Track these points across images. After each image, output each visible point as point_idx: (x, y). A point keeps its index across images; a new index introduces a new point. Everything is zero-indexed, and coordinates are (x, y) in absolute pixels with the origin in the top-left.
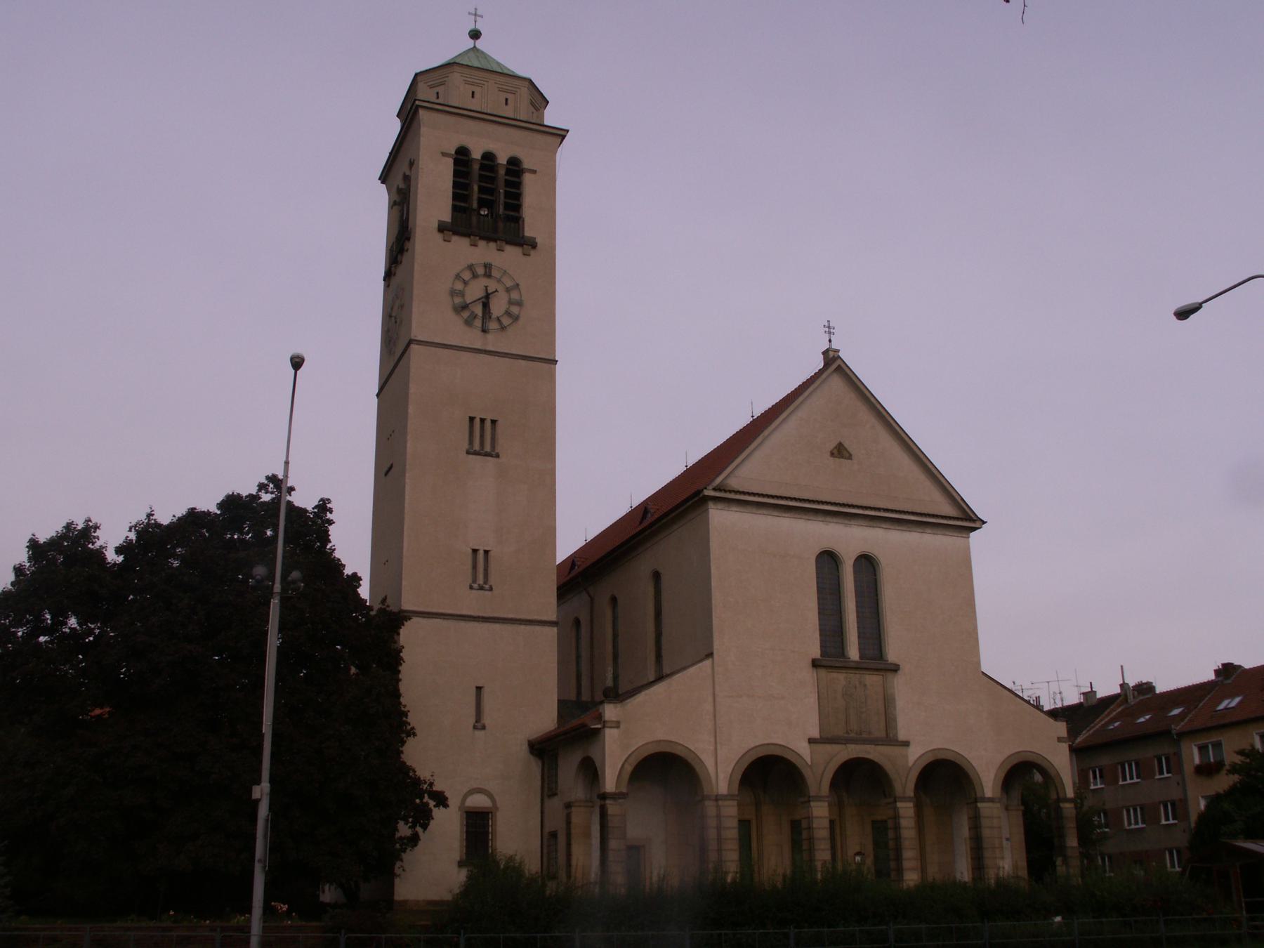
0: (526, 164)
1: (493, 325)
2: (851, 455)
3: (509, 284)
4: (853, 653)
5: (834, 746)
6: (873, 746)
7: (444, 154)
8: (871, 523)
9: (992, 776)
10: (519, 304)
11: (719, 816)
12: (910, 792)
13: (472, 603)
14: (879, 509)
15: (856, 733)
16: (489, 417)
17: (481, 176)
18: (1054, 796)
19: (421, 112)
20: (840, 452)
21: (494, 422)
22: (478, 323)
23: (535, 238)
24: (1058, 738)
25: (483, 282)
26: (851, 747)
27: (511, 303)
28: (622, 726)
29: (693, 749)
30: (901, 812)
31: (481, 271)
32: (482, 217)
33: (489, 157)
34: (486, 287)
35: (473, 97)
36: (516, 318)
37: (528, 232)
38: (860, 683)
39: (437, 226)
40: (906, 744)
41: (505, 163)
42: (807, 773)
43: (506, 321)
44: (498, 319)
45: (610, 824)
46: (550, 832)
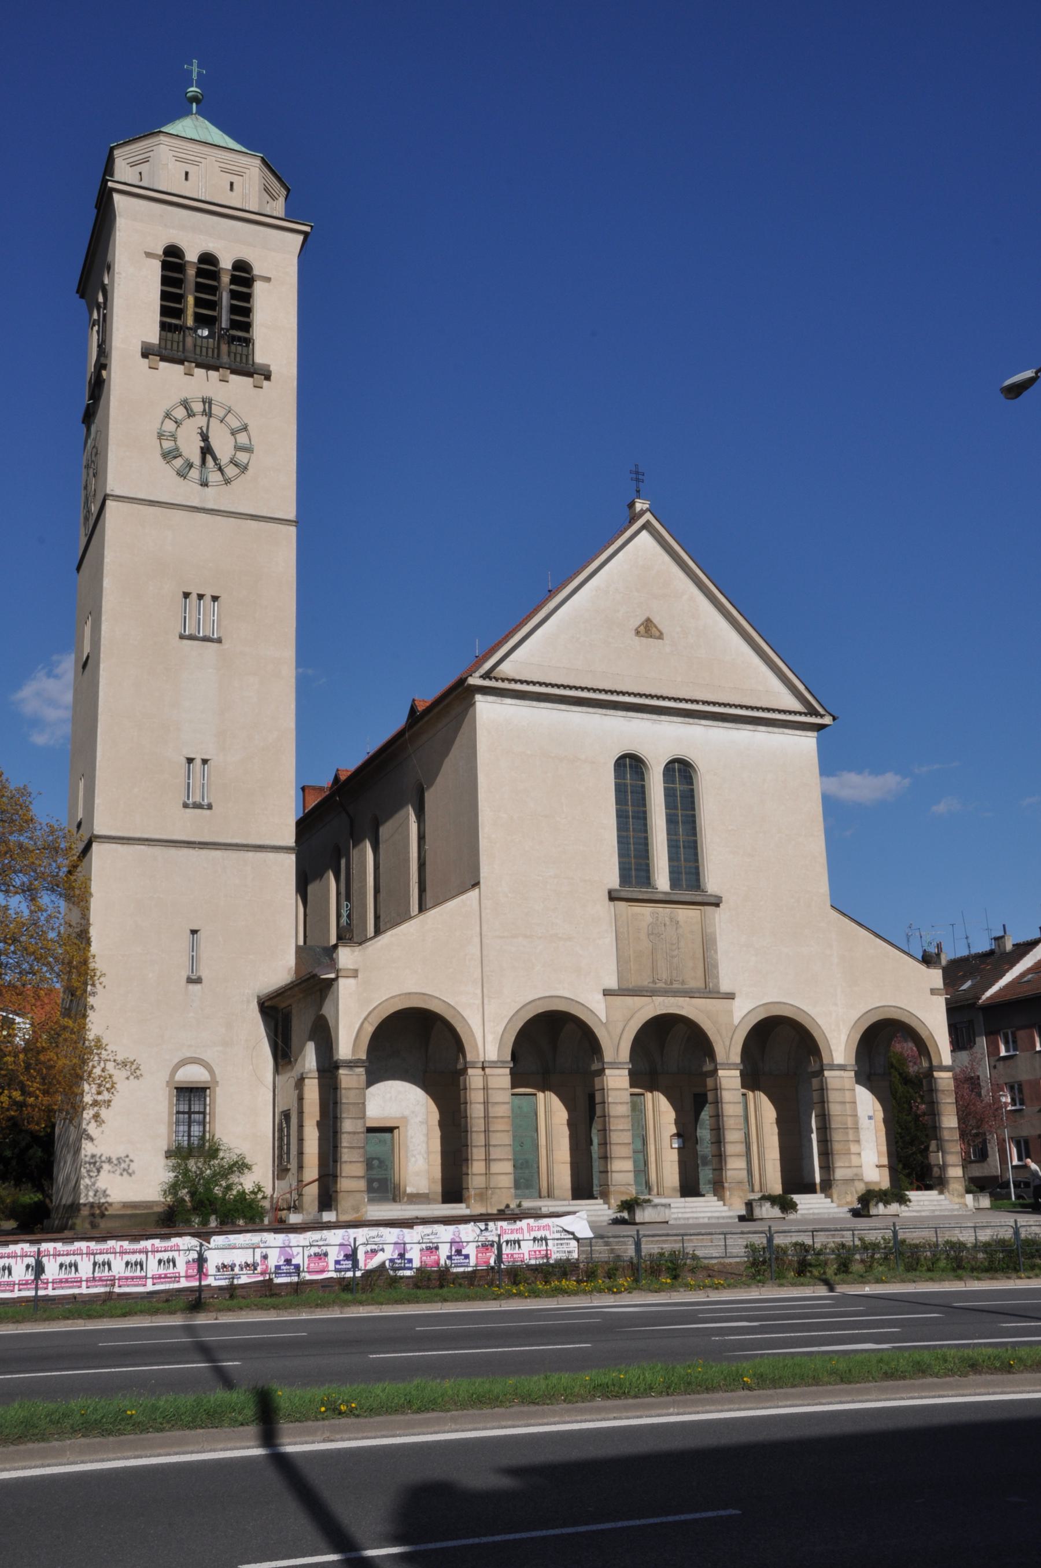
0: (256, 271)
2: (661, 634)
3: (235, 424)
4: (662, 881)
6: (688, 999)
7: (149, 255)
8: (687, 720)
9: (844, 1038)
10: (248, 449)
11: (486, 1088)
12: (736, 1057)
14: (697, 702)
15: (666, 983)
16: (209, 593)
17: (198, 284)
19: (116, 197)
20: (648, 629)
22: (194, 473)
23: (269, 366)
24: (932, 990)
26: (658, 999)
27: (238, 448)
29: (452, 1004)
31: (198, 407)
33: (208, 259)
35: (187, 179)
36: (244, 468)
37: (260, 357)
38: (671, 919)
40: (731, 996)
41: (230, 267)
43: (231, 471)
45: (344, 1101)
46: (282, 1112)
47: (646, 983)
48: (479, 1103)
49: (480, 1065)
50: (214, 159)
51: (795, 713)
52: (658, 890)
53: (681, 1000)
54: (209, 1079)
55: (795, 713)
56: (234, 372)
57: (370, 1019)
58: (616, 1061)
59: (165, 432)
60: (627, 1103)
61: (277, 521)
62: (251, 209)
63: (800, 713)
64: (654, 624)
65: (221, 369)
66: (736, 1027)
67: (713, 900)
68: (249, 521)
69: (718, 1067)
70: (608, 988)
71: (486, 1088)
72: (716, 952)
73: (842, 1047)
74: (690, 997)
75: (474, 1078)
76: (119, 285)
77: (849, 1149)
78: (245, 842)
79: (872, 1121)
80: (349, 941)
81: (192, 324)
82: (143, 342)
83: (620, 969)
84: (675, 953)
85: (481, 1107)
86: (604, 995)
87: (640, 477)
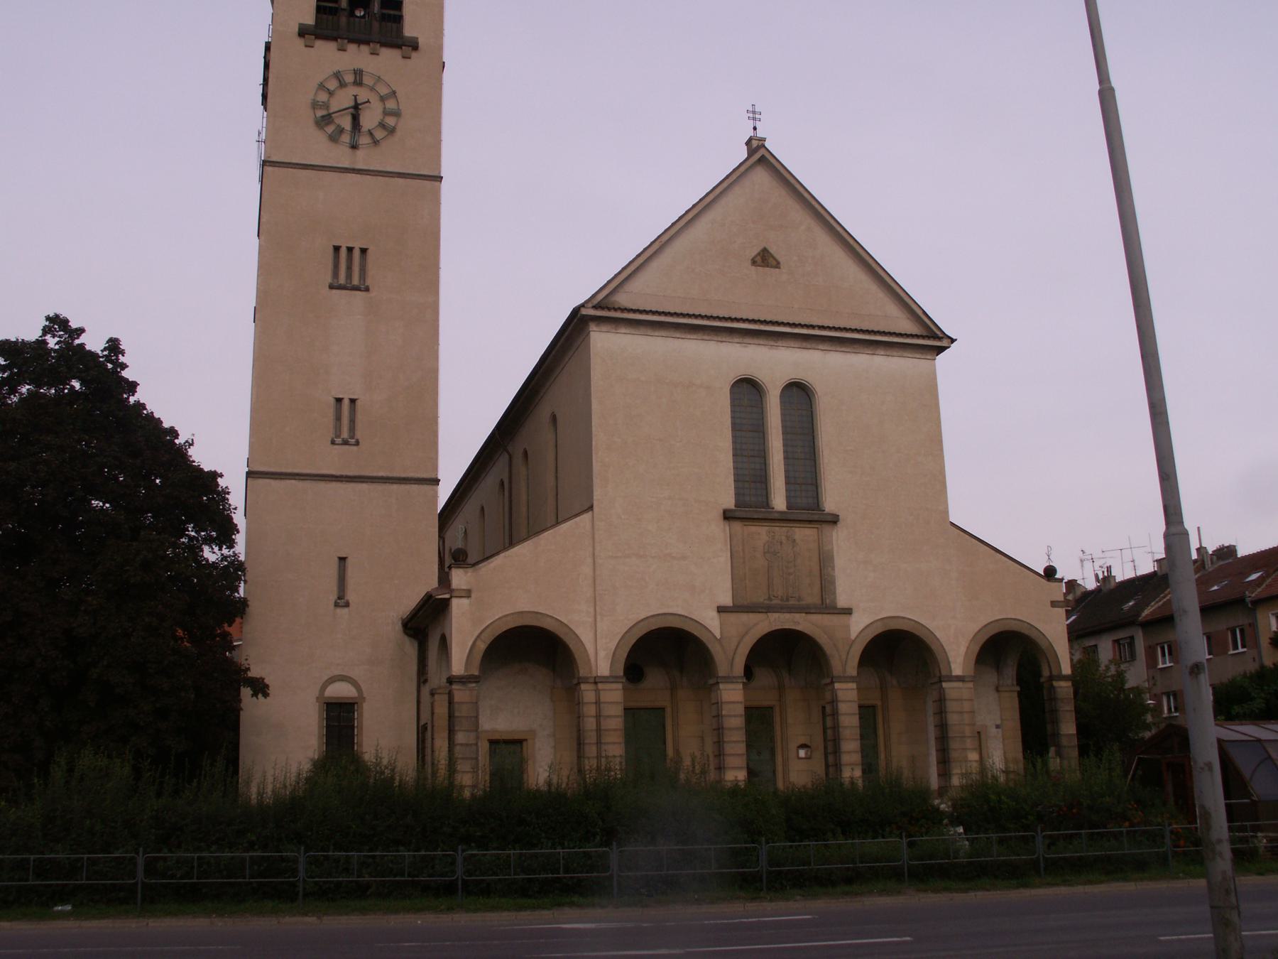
1: (364, 140)
2: (778, 263)
3: (384, 91)
4: (779, 502)
5: (752, 615)
6: (804, 615)
8: (804, 344)
9: (963, 650)
10: (396, 114)
11: (598, 703)
12: (852, 669)
13: (333, 460)
14: (812, 327)
15: (782, 600)
16: (357, 245)
18: (1046, 673)
20: (765, 259)
22: (346, 138)
23: (417, 38)
25: (353, 90)
27: (387, 113)
28: (473, 595)
29: (566, 622)
30: (841, 695)
31: (349, 78)
32: (357, 20)
34: (355, 96)
36: (392, 131)
38: (788, 537)
39: (297, 30)
40: (848, 612)
42: (715, 649)
43: (379, 134)
44: (370, 133)
47: (761, 600)
48: (591, 716)
49: (592, 680)
51: (912, 336)
52: (774, 510)
53: (797, 616)
54: (356, 695)
55: (912, 336)
56: (384, 45)
57: (482, 637)
58: (731, 675)
60: (741, 715)
63: (917, 336)
64: (771, 254)
66: (854, 641)
67: (829, 518)
68: (396, 179)
69: (834, 680)
70: (722, 605)
71: (598, 703)
72: (833, 569)
73: (960, 659)
74: (806, 613)
75: (587, 692)
77: (967, 757)
78: (390, 475)
79: (1000, 730)
80: (462, 563)
81: (345, 5)
82: (300, 24)
83: (734, 586)
84: (791, 571)
85: (594, 720)
86: (719, 612)
87: (757, 116)
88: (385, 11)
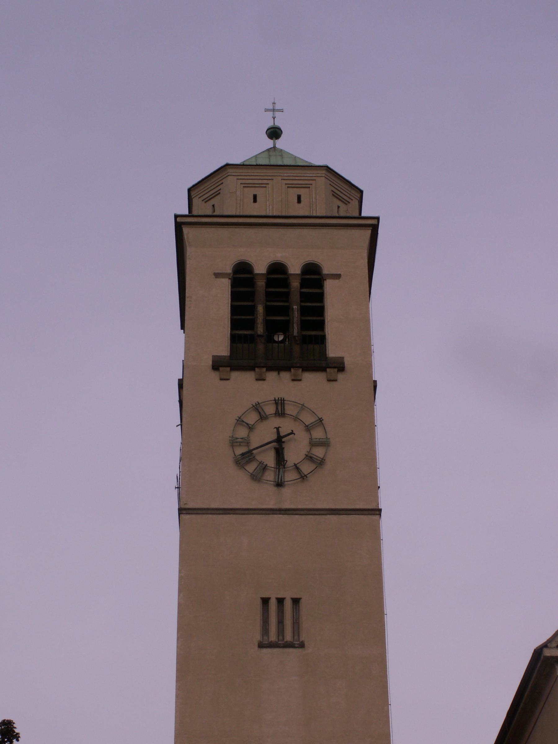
0: (325, 271)
1: (290, 476)
3: (309, 419)
7: (218, 275)
10: (325, 443)
16: (288, 596)
21: (296, 601)
22: (270, 476)
23: (343, 358)
25: (276, 422)
27: (313, 444)
31: (270, 409)
32: (275, 345)
36: (320, 463)
39: (211, 363)
43: (306, 468)
44: (296, 467)
50: (280, 178)
59: (237, 439)
61: (359, 512)
62: (318, 215)
65: (292, 369)
68: (328, 516)
76: (190, 307)
81: (262, 331)
82: (213, 356)
88: (304, 333)
